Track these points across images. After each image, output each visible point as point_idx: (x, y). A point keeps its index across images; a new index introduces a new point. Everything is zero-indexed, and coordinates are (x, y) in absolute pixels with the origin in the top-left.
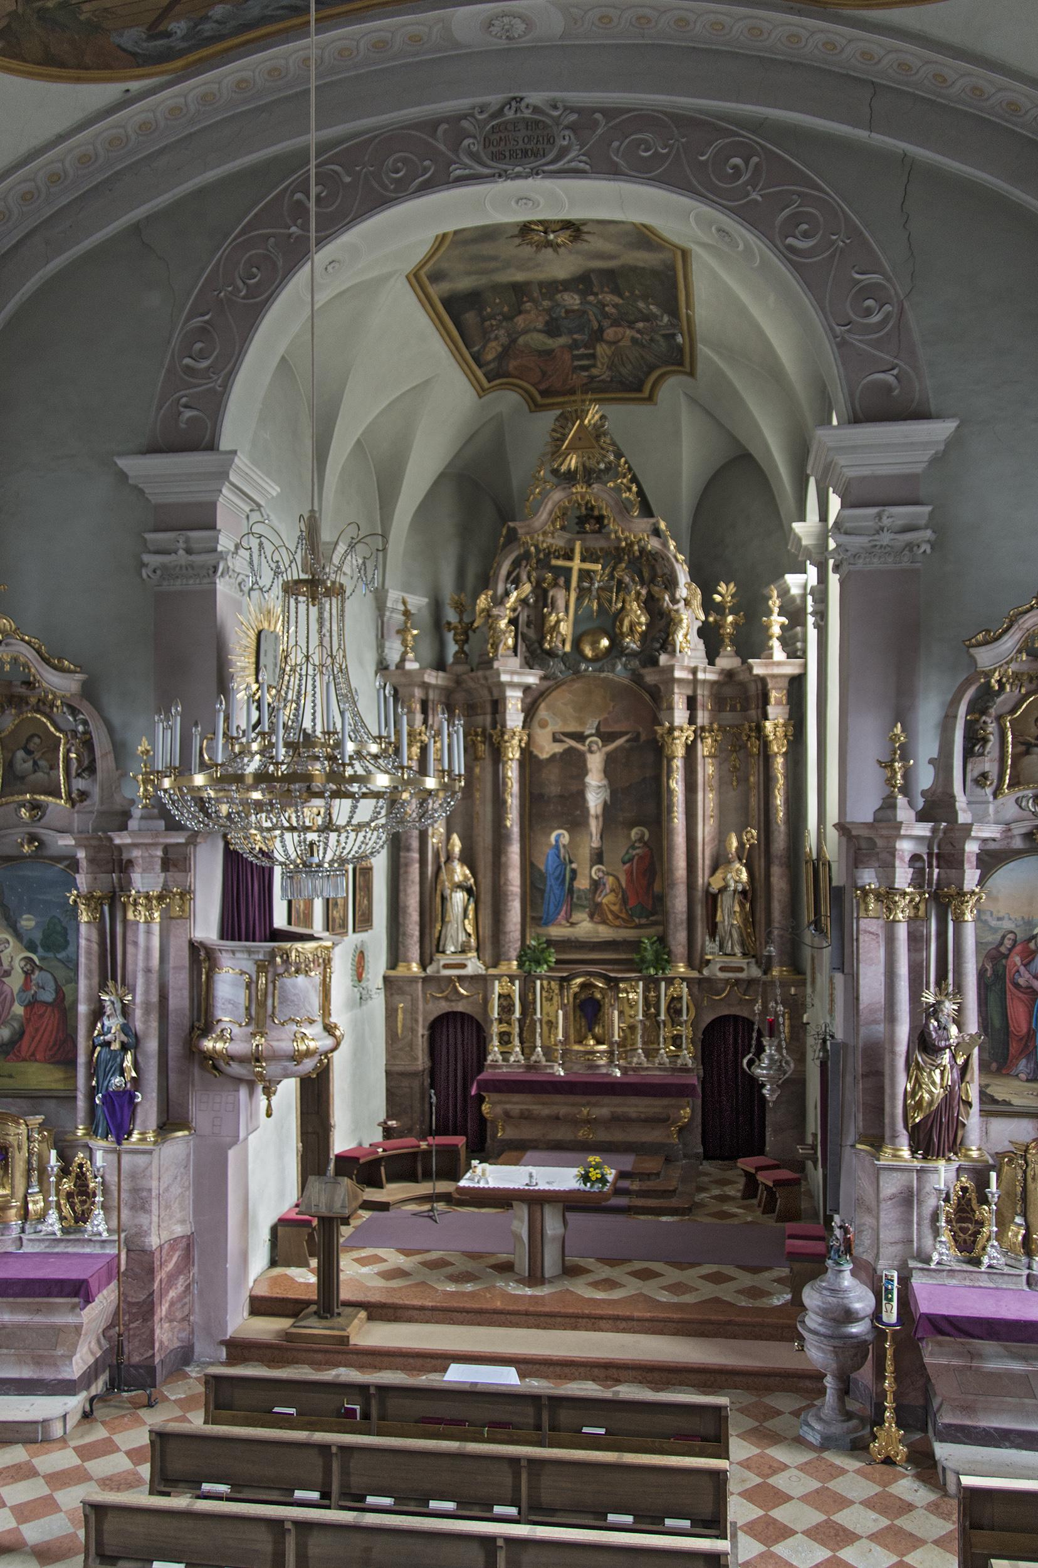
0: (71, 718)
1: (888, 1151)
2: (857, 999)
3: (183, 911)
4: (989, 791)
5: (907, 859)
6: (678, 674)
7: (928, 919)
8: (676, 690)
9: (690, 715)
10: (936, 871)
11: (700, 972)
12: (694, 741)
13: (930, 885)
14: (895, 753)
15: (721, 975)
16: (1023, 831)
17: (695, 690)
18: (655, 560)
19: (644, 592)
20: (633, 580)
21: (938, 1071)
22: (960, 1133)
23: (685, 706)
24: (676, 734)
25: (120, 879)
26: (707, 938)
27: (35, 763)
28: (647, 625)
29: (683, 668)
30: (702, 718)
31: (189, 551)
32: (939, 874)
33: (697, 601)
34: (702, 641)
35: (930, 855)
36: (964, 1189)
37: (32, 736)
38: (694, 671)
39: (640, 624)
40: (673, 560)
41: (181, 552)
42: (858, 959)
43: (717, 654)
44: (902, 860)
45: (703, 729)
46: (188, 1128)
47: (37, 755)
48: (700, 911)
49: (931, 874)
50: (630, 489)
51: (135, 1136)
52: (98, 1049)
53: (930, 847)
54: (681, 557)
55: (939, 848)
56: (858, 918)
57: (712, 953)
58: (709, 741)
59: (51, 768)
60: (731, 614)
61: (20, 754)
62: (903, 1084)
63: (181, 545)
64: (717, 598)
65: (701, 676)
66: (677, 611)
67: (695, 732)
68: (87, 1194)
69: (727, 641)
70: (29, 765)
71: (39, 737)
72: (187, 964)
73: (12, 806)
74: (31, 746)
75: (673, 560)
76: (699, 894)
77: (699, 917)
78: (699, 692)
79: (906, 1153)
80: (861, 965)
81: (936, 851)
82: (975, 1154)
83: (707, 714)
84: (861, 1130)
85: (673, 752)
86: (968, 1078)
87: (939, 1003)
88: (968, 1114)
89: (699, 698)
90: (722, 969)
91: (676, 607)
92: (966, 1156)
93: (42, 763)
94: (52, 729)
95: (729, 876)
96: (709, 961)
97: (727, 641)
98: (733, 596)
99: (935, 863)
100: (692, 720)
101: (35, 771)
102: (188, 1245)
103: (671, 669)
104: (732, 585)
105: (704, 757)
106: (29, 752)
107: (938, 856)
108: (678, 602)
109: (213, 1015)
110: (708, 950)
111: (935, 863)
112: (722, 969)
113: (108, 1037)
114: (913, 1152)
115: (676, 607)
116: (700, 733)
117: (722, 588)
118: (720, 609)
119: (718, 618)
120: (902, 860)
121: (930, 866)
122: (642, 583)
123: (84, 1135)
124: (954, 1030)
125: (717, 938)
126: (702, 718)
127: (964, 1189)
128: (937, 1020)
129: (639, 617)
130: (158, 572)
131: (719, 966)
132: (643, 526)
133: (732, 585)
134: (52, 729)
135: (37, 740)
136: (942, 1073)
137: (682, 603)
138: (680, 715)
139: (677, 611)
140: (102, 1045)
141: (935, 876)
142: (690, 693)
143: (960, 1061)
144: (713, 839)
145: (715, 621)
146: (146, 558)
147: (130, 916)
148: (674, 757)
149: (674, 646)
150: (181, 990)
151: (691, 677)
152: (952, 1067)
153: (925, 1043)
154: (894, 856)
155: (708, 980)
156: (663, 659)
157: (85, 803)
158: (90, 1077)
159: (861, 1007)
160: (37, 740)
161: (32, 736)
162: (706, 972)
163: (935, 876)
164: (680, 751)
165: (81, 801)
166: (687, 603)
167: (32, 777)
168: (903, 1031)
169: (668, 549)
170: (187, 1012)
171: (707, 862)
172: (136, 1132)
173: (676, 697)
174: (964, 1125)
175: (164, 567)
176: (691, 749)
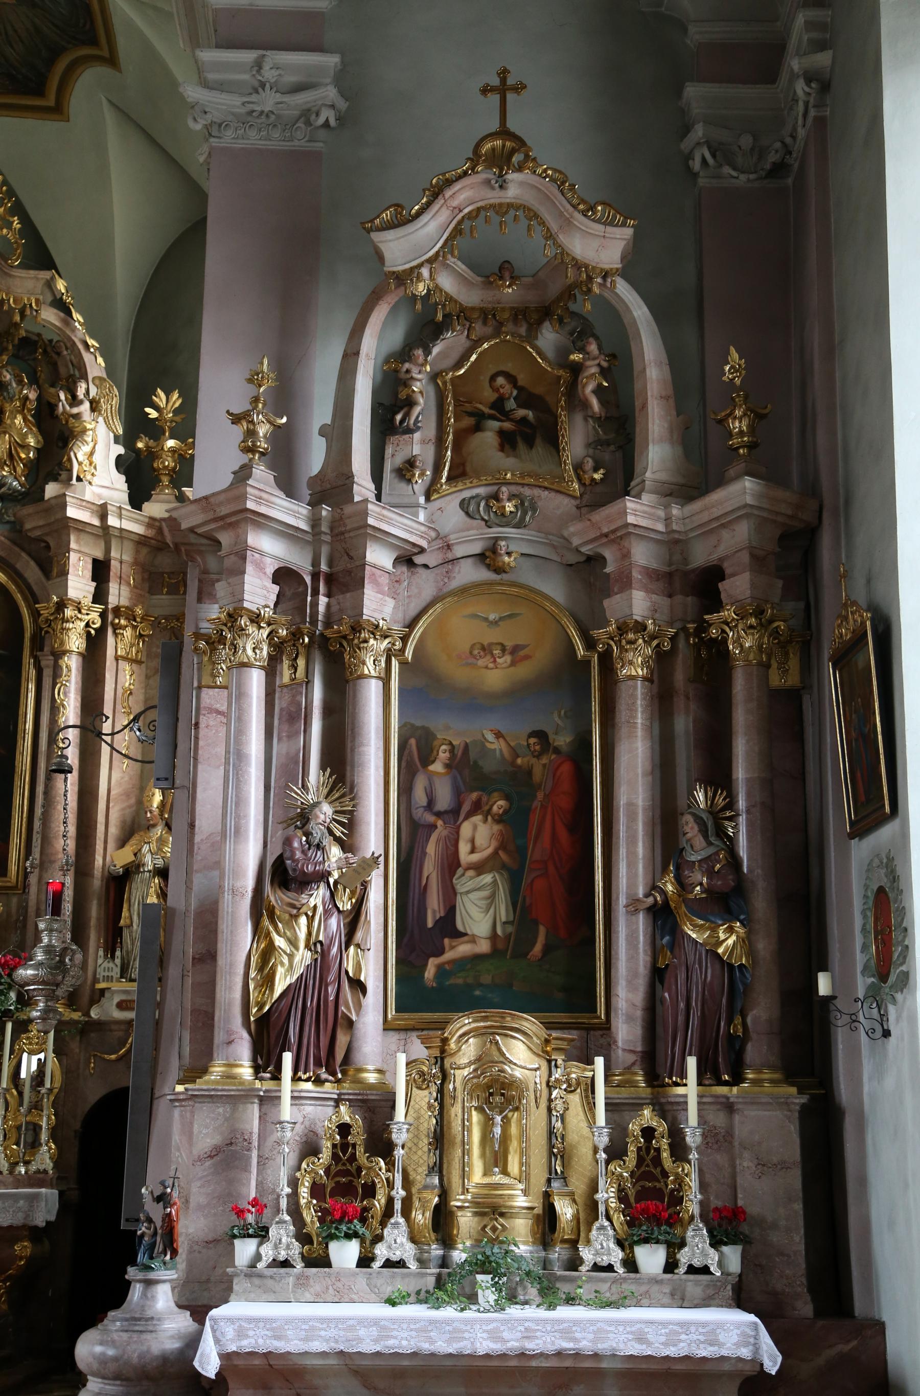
1: (217, 1070)
2: (192, 825)
4: (420, 484)
5: (270, 570)
6: (71, 512)
7: (309, 682)
8: (73, 545)
9: (96, 588)
10: (323, 600)
11: (87, 1014)
12: (102, 631)
13: (314, 621)
14: (256, 400)
15: (118, 1015)
16: (477, 548)
17: (108, 551)
18: (59, 354)
19: (33, 395)
20: (20, 382)
21: (303, 920)
22: (342, 1040)
23: (89, 574)
24: (69, 612)
26: (101, 953)
28: (38, 451)
29: (84, 504)
30: (118, 594)
32: (328, 606)
33: (113, 401)
34: (123, 478)
35: (315, 576)
36: (344, 1129)
38: (102, 512)
39: (25, 447)
40: (81, 347)
42: (196, 759)
43: (148, 498)
44: (260, 567)
45: (117, 611)
48: (94, 911)
49: (315, 604)
50: (9, 225)
53: (316, 563)
54: (91, 342)
55: (330, 564)
56: (200, 688)
57: (109, 979)
58: (128, 633)
60: (171, 438)
62: (239, 940)
64: (153, 414)
65: (112, 521)
66: (77, 416)
67: (103, 615)
69: (166, 480)
75: (81, 347)
76: (97, 883)
77: (93, 922)
78: (114, 554)
79: (246, 1072)
80: (200, 767)
81: (324, 567)
82: (371, 1078)
83: (125, 592)
84: (187, 1060)
85: (62, 643)
86: (359, 936)
87: (316, 804)
88: (359, 1006)
89: (114, 564)
90: (121, 1006)
91: (75, 410)
92: (360, 1082)
95: (146, 848)
96: (102, 992)
97: (166, 480)
98: (176, 412)
99: (322, 588)
100: (100, 596)
103: (61, 503)
104: (176, 395)
105: (117, 658)
107: (330, 579)
108: (81, 402)
110: (101, 973)
111: (322, 588)
112: (121, 1006)
114: (257, 1069)
115: (75, 410)
116: (111, 618)
117: (160, 398)
118: (154, 430)
119: (152, 443)
120: (260, 567)
121: (316, 592)
122: (34, 381)
124: (335, 852)
125: (118, 953)
126: (118, 594)
127: (344, 1129)
128: (308, 834)
129: (24, 436)
131: (116, 1000)
132: (30, 284)
133: (176, 395)
136: (310, 920)
137: (86, 406)
138: (79, 584)
139: (77, 416)
141: (322, 608)
142: (99, 555)
143: (345, 904)
144: (127, 795)
145: (147, 446)
148: (65, 652)
149: (70, 470)
151: (96, 522)
152: (327, 913)
153: (284, 875)
154: (244, 558)
155: (99, 1026)
156: (51, 490)
159: (197, 839)
162: (94, 1014)
163: (322, 608)
164: (75, 642)
166: (95, 406)
168: (249, 855)
169: (74, 329)
171: (113, 830)
173: (73, 557)
174: (350, 1024)
176: (95, 643)
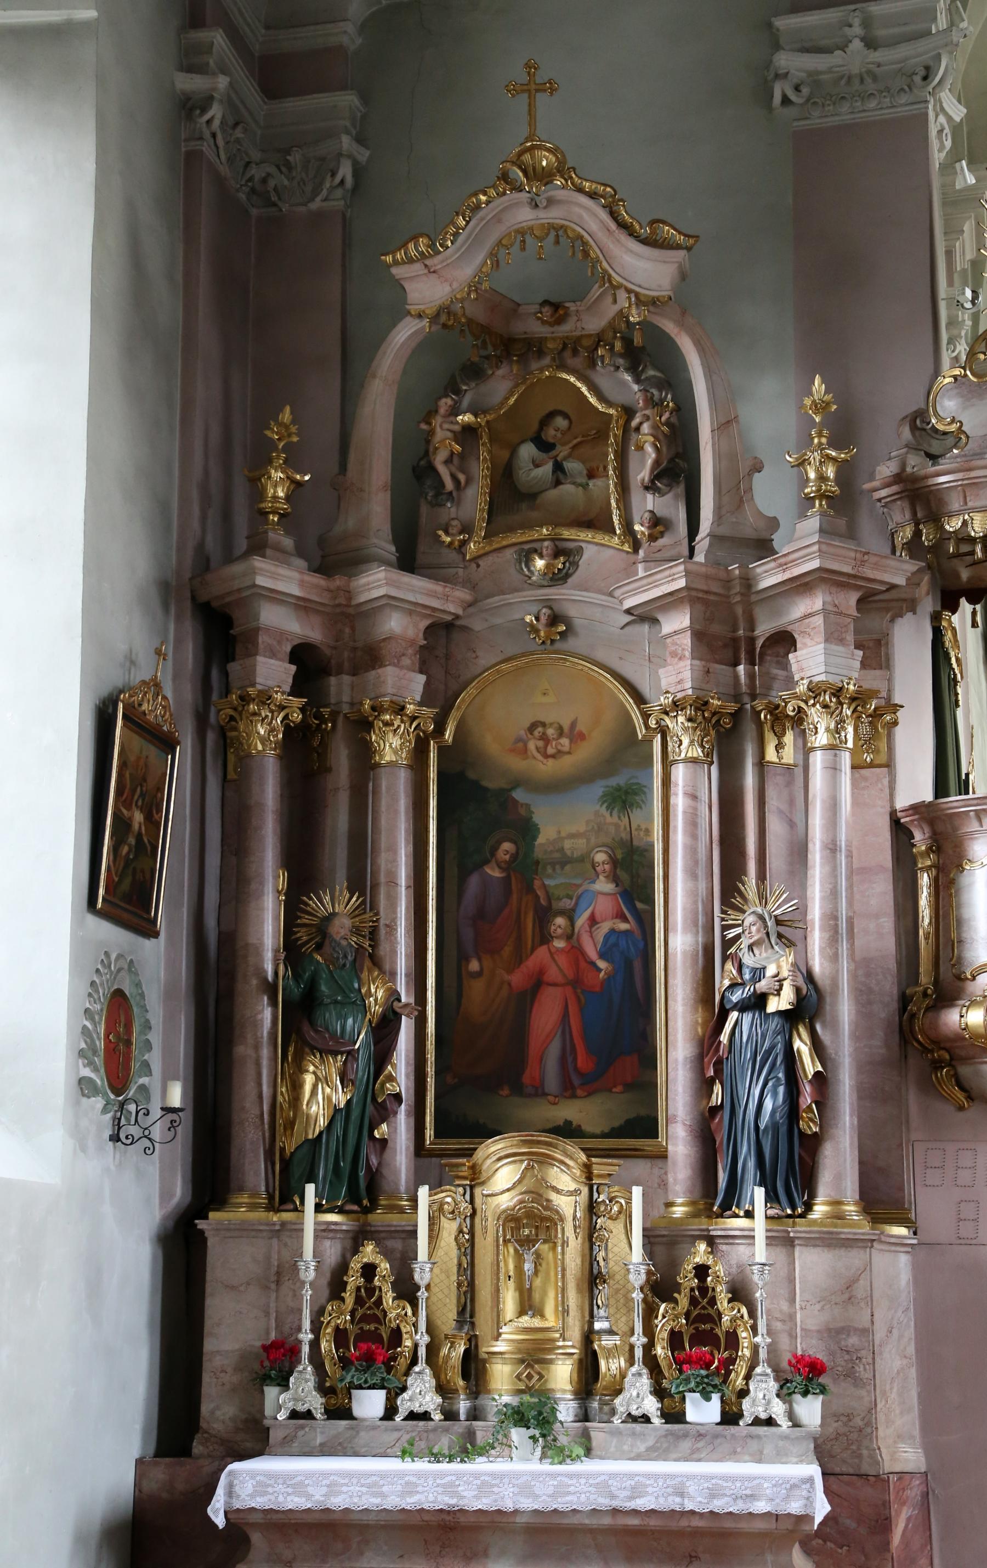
0: (628, 378)
3: (876, 751)
25: (751, 676)
27: (558, 467)
31: (871, 43)
37: (552, 415)
41: (857, 44)
46: (903, 1220)
47: (562, 452)
51: (820, 1210)
52: (734, 1015)
59: (591, 475)
61: (527, 451)
63: (857, 30)
68: (709, 1338)
70: (548, 467)
71: (566, 416)
72: (888, 863)
73: (510, 554)
74: (550, 434)
93: (572, 466)
94: (593, 400)
101: (558, 483)
102: (926, 1495)
106: (545, 446)
109: (960, 961)
113: (762, 986)
123: (694, 1215)
130: (805, 91)
134: (593, 400)
135: (561, 422)
140: (743, 1007)
146: (784, 60)
147: (771, 755)
150: (877, 916)
157: (661, 542)
158: (704, 1086)
160: (561, 422)
161: (552, 415)
165: (652, 538)
167: (553, 494)
170: (892, 965)
172: (819, 1200)
175: (814, 79)
